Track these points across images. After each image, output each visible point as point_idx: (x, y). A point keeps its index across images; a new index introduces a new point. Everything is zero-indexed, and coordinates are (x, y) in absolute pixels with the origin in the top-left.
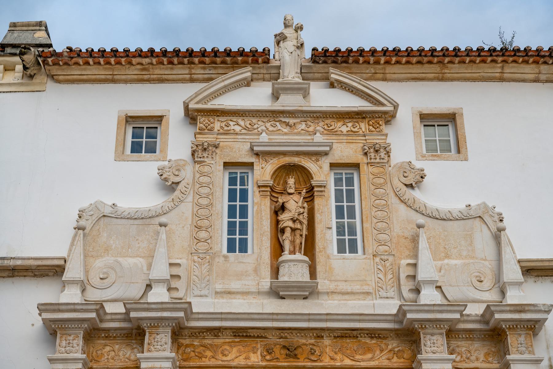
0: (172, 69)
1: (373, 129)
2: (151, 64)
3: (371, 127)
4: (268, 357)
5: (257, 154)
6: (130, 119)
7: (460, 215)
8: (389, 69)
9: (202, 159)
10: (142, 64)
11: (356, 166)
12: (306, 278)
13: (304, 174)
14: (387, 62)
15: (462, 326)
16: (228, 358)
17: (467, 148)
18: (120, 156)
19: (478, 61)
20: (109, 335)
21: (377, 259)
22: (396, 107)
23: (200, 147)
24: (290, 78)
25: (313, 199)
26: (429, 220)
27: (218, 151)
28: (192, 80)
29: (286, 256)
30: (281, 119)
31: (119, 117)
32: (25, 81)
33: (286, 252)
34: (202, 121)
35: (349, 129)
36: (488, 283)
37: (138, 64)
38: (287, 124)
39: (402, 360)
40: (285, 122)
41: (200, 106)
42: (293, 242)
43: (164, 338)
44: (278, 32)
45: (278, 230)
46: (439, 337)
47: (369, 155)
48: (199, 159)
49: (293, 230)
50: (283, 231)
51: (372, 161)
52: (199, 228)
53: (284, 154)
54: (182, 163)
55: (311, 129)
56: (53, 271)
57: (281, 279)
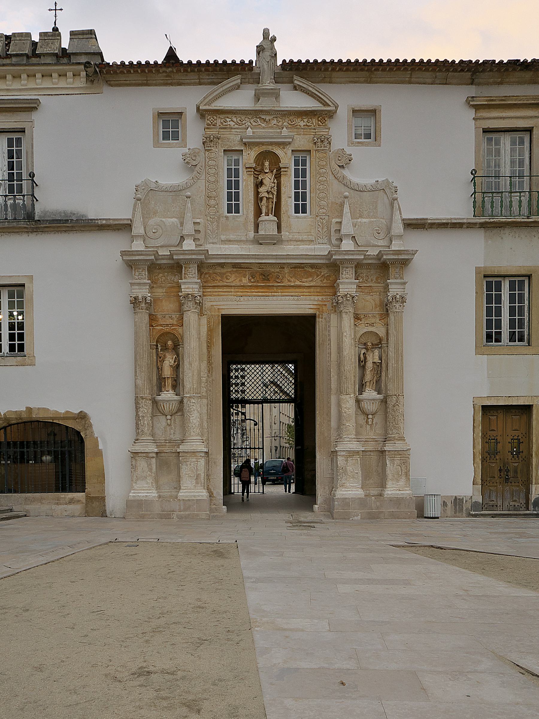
0: (186, 75)
2: (173, 72)
3: (319, 122)
4: (252, 280)
5: (245, 144)
6: (160, 114)
7: (371, 188)
8: (334, 74)
9: (210, 148)
12: (276, 233)
13: (275, 159)
15: (365, 262)
16: (230, 281)
18: (156, 144)
19: (395, 69)
20: (161, 267)
21: (318, 218)
22: (337, 107)
23: (208, 139)
24: (267, 84)
26: (352, 191)
27: (219, 141)
28: (200, 84)
29: (263, 217)
30: (261, 116)
32: (89, 85)
33: (263, 214)
34: (209, 119)
36: (382, 235)
37: (163, 72)
38: (265, 120)
39: (329, 281)
41: (207, 107)
42: (267, 207)
43: (193, 270)
44: (258, 44)
45: (258, 199)
46: (350, 269)
48: (208, 148)
49: (268, 199)
50: (261, 199)
52: (209, 197)
53: (263, 144)
54: (197, 151)
55: (280, 124)
56: (123, 227)
57: (261, 232)
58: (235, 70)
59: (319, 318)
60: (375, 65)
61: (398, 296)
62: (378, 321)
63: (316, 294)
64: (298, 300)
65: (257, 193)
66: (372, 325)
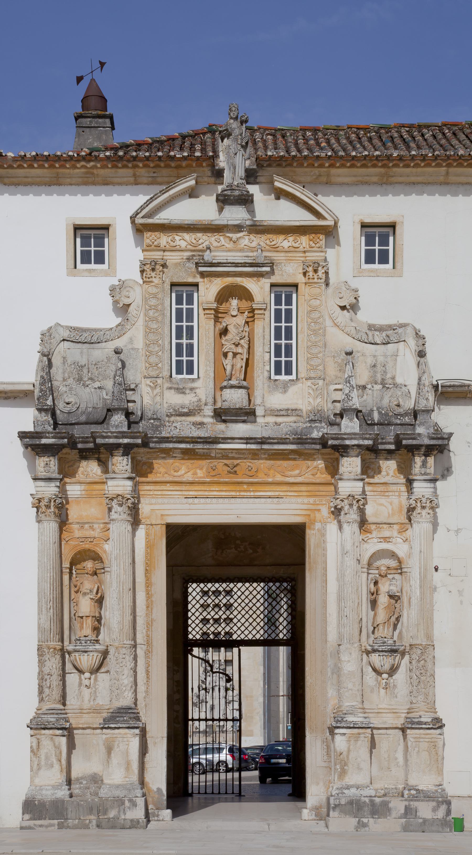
1: (313, 245)
3: (311, 243)
6: (77, 228)
8: (333, 171)
9: (150, 280)
10: (86, 167)
11: (296, 286)
14: (331, 166)
17: (402, 263)
25: (254, 321)
31: (67, 225)
34: (149, 237)
35: (290, 244)
37: (83, 167)
40: (229, 237)
47: (307, 274)
48: (148, 280)
50: (225, 355)
51: (311, 281)
58: (187, 166)
59: (310, 528)
60: (393, 160)
61: (424, 500)
62: (395, 534)
63: (305, 494)
64: (278, 503)
65: (218, 346)
66: (386, 539)
